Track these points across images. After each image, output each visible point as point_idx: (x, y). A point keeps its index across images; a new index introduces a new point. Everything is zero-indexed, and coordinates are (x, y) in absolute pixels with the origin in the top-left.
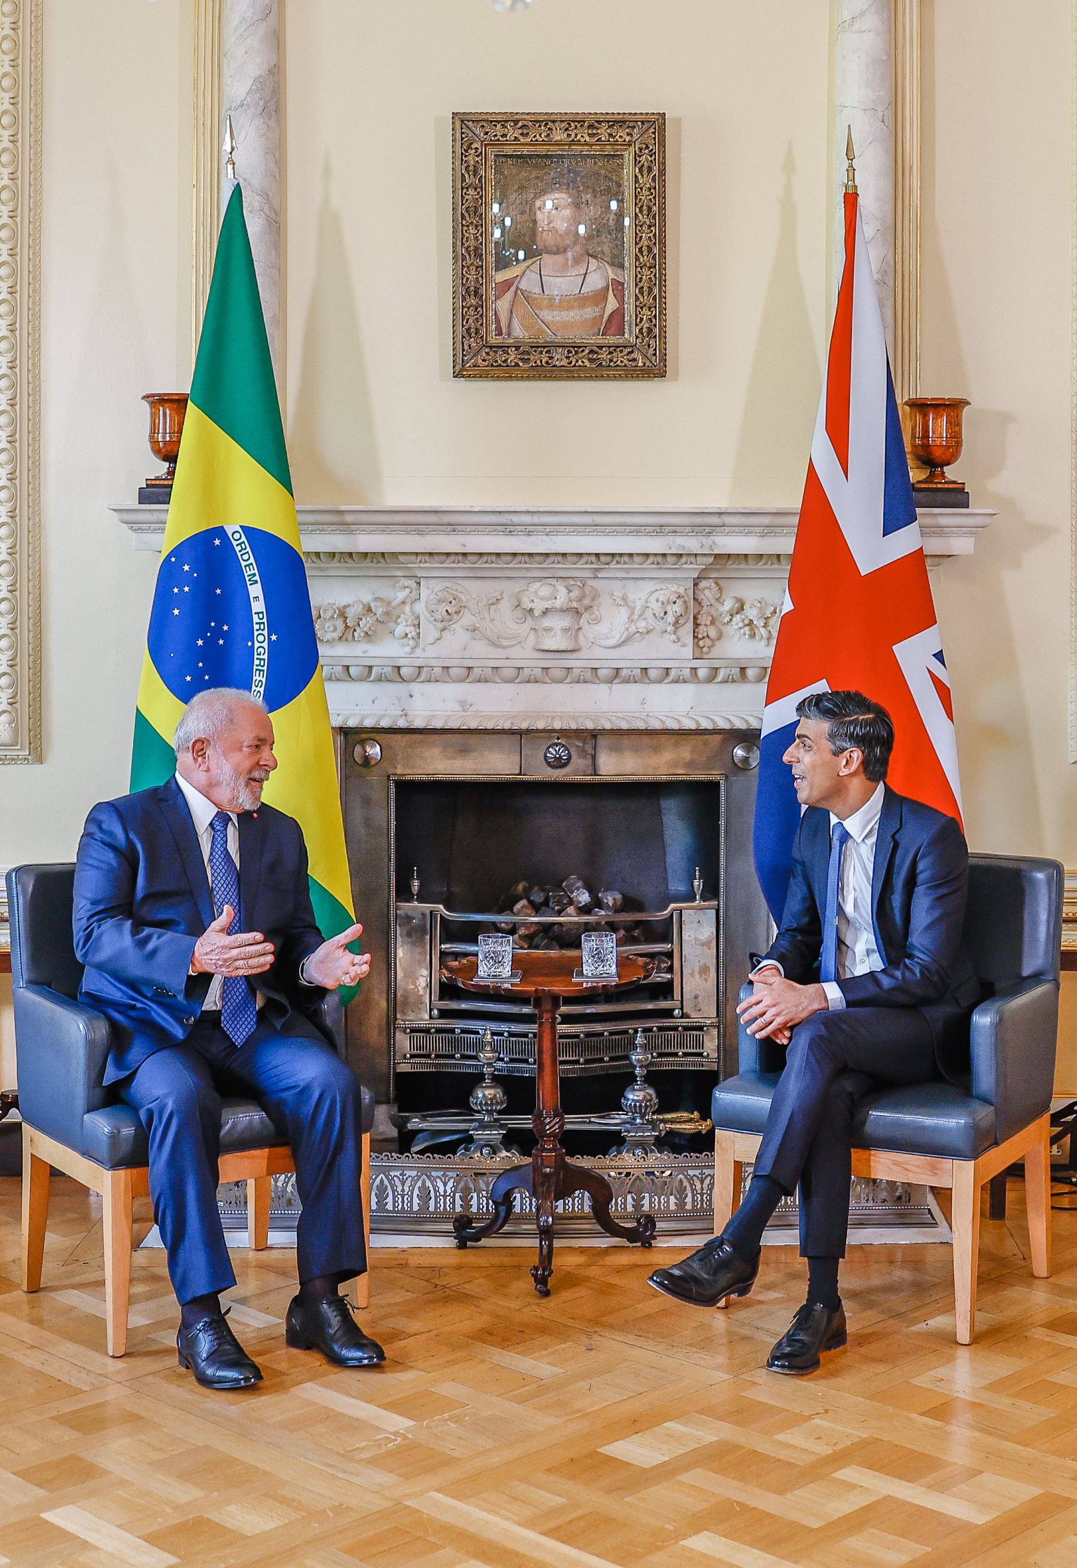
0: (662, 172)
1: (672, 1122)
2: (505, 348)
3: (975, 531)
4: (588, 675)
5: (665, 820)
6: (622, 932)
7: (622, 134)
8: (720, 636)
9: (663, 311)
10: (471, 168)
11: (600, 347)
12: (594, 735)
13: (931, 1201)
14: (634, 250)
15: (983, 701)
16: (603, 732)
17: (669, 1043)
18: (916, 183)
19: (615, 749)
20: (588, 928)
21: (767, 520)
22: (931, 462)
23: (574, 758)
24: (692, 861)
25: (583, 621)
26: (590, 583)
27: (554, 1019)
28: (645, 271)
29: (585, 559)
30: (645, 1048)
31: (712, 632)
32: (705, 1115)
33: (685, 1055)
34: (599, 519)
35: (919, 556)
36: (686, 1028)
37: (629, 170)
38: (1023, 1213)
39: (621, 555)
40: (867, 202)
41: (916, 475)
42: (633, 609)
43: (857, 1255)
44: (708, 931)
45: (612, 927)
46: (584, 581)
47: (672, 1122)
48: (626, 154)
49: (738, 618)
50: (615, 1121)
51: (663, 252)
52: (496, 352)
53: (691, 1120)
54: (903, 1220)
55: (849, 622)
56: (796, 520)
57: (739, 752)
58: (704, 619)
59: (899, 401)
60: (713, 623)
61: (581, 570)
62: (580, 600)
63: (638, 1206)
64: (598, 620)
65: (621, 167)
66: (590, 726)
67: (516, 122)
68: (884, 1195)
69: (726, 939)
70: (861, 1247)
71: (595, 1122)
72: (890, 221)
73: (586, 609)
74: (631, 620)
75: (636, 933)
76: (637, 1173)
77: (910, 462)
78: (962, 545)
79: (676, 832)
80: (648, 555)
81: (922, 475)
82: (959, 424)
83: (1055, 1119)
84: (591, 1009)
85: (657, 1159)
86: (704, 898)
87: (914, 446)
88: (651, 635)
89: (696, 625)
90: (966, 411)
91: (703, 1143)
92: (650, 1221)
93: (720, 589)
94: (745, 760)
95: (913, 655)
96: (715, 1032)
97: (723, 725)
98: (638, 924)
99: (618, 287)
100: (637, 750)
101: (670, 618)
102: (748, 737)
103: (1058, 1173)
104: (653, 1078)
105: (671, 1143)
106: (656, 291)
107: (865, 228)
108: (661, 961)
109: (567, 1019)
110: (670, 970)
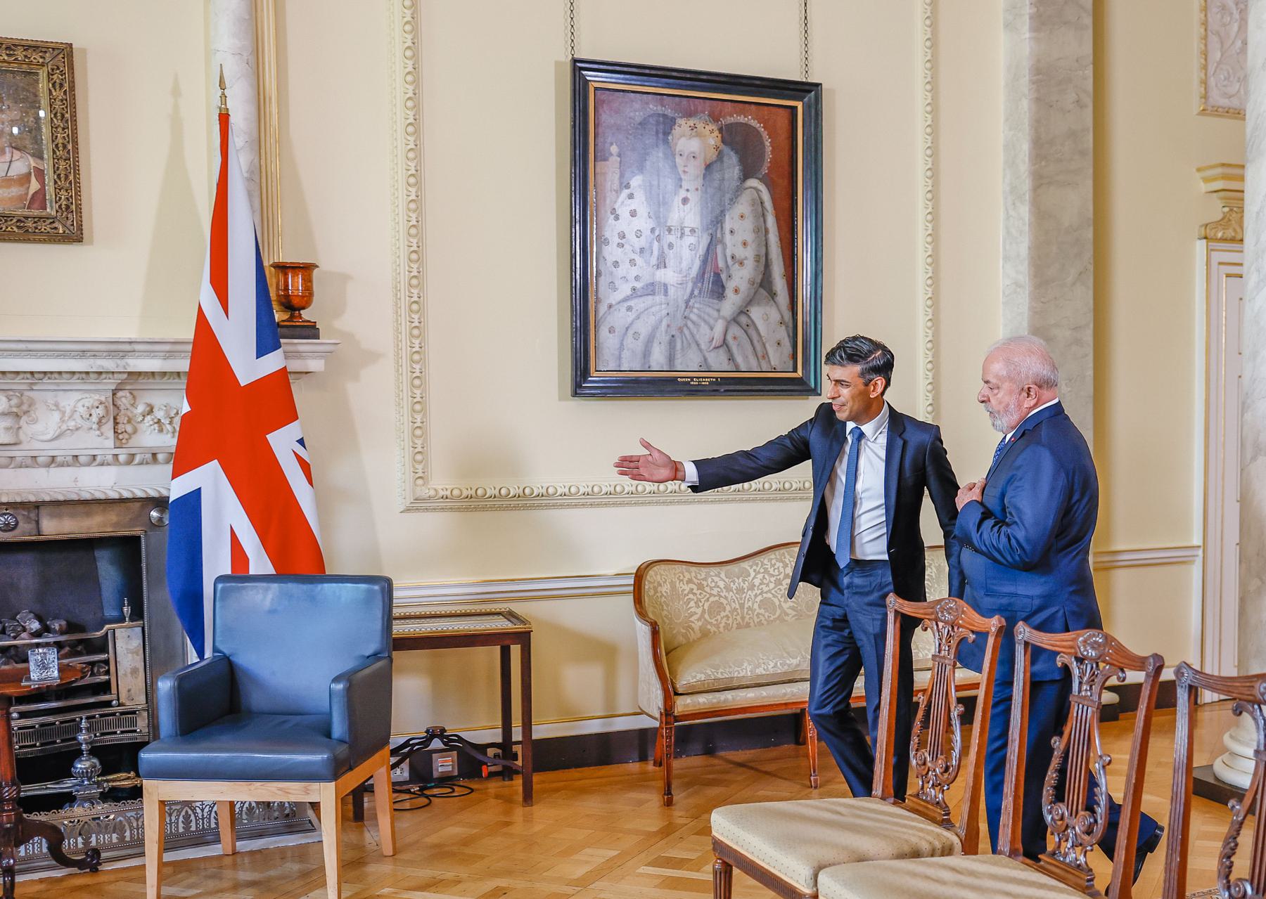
0: (72, 88)
1: (113, 781)
3: (327, 355)
4: (29, 461)
5: (99, 564)
6: (67, 649)
7: (36, 57)
8: (135, 431)
9: (78, 193)
11: (27, 218)
12: (37, 506)
13: (311, 814)
14: (51, 146)
15: (336, 472)
16: (44, 503)
17: (109, 724)
18: (274, 109)
19: (52, 516)
20: (38, 645)
21: (167, 347)
22: (291, 306)
23: (21, 524)
24: (122, 595)
25: (23, 422)
26: (27, 393)
27: (9, 714)
28: (62, 163)
29: (21, 376)
30: (88, 729)
31: (129, 428)
32: (138, 775)
33: (122, 732)
34: (31, 346)
35: (283, 372)
36: (122, 714)
37: (43, 85)
38: (375, 817)
39: (52, 373)
40: (236, 121)
41: (279, 316)
42: (64, 413)
43: (258, 856)
44: (137, 642)
45: (59, 645)
46: (21, 393)
47: (113, 781)
48: (40, 72)
49: (148, 418)
50: (67, 785)
51: (76, 149)
53: (128, 778)
54: (291, 829)
55: (231, 419)
56: (190, 347)
57: (154, 514)
58: (121, 419)
59: (266, 264)
60: (129, 421)
61: (19, 384)
62: (19, 406)
63: (87, 842)
64: (35, 421)
65: (37, 81)
66: (32, 499)
68: (276, 814)
69: (151, 649)
70: (260, 851)
71: (52, 788)
72: (255, 135)
73: (25, 413)
74: (62, 420)
75: (79, 648)
76: (86, 819)
77: (275, 306)
78: (315, 365)
79: (108, 572)
80: (74, 373)
81: (286, 316)
82: (311, 281)
83: (394, 752)
84: (42, 706)
85: (100, 808)
86: (131, 620)
87: (278, 296)
88: (79, 432)
89: (116, 423)
90: (316, 272)
91: (136, 793)
92: (96, 852)
93: (134, 397)
94: (160, 519)
95: (282, 442)
96: (145, 714)
97: (140, 494)
98: (80, 642)
99: (40, 174)
100: (72, 516)
101: (95, 419)
102: (160, 503)
103: (397, 787)
104: (95, 751)
105: (113, 795)
106: (71, 177)
107: (236, 139)
108: (100, 667)
109: (23, 715)
110: (108, 673)
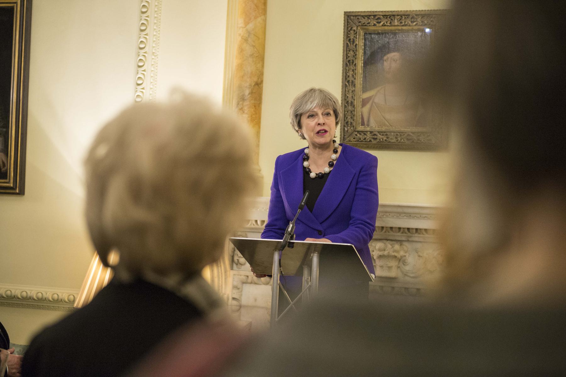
2: (364, 133)
10: (352, 40)
52: (360, 134)
67: (375, 16)
